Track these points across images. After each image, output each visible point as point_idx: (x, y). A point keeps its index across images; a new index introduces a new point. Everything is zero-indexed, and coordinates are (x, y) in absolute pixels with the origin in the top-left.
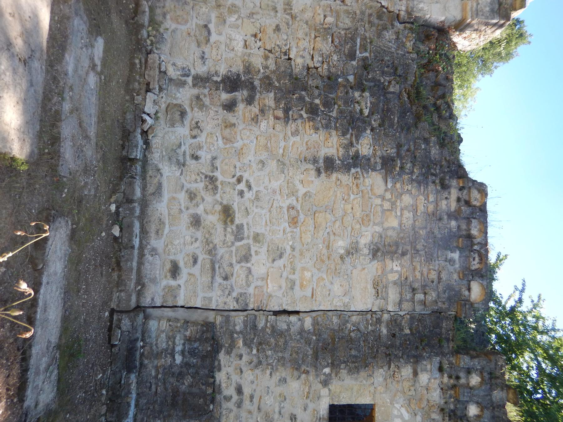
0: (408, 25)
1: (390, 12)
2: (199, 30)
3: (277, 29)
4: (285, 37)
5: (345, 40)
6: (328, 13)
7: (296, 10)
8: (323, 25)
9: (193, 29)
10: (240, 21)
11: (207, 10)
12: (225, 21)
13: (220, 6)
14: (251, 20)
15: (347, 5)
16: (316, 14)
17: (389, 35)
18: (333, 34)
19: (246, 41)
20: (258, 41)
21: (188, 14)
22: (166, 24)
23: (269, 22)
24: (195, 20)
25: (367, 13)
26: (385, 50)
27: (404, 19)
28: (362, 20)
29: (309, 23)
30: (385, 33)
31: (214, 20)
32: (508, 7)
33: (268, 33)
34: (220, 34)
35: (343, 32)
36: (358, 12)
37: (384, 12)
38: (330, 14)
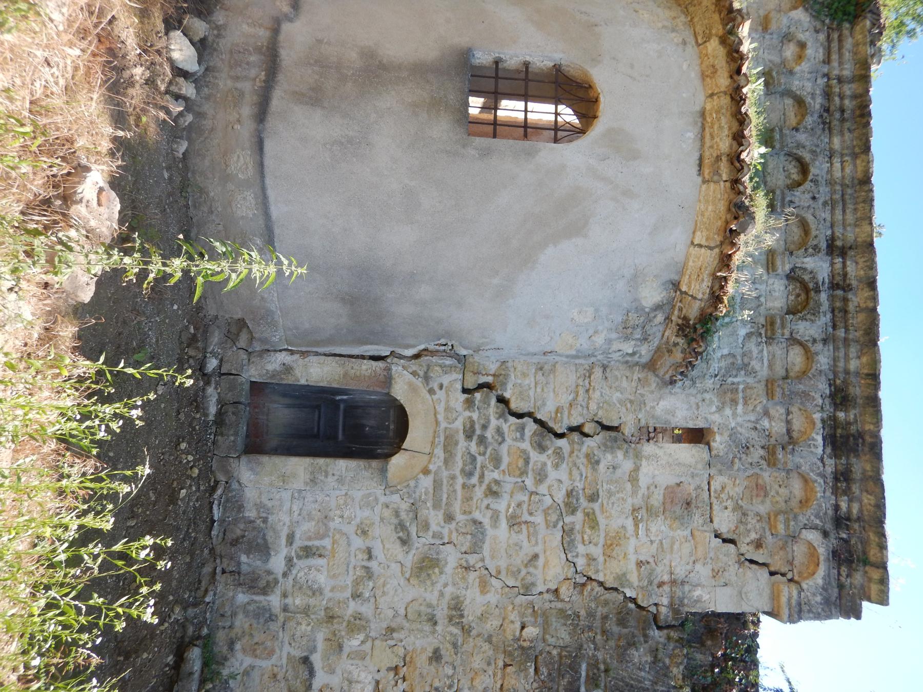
0: (674, 634)
1: (639, 607)
2: (293, 667)
3: (436, 656)
4: (450, 672)
5: (559, 669)
6: (529, 619)
7: (470, 617)
8: (519, 640)
9: (282, 666)
10: (369, 644)
11: (309, 628)
12: (340, 647)
13: (332, 617)
14: (389, 642)
15: (562, 601)
16: (507, 621)
17: (640, 655)
18: (536, 657)
19: (378, 682)
20: (400, 681)
21: (275, 637)
22: (233, 660)
23: (420, 642)
24: (287, 648)
25: (599, 614)
26: (632, 686)
27: (666, 622)
28: (590, 628)
29: (494, 639)
30: (633, 651)
31: (320, 645)
32: (856, 591)
33: (418, 665)
34: (332, 672)
35: (555, 652)
36: (583, 613)
37: (631, 610)
38: (533, 620)
